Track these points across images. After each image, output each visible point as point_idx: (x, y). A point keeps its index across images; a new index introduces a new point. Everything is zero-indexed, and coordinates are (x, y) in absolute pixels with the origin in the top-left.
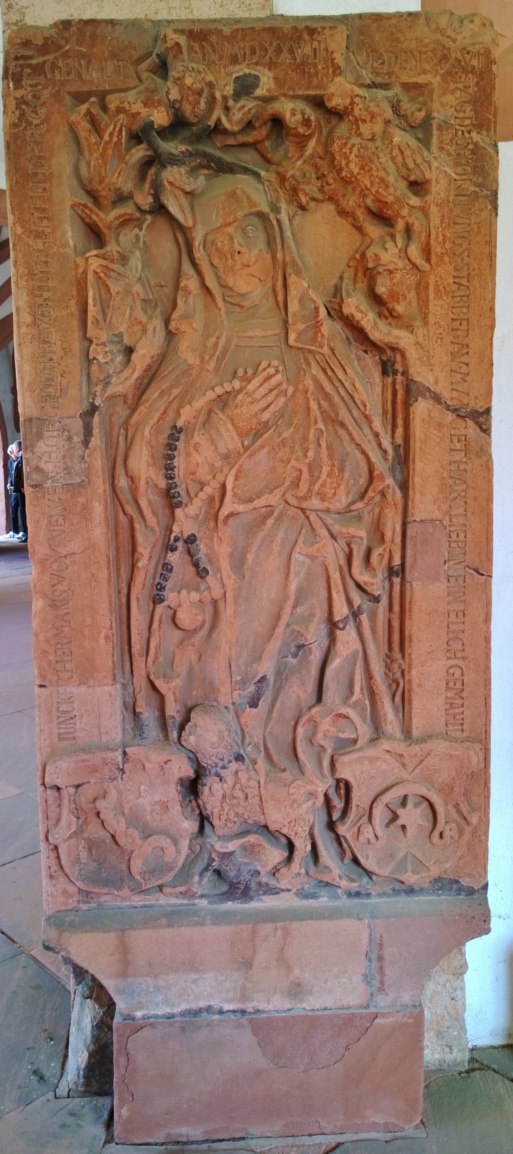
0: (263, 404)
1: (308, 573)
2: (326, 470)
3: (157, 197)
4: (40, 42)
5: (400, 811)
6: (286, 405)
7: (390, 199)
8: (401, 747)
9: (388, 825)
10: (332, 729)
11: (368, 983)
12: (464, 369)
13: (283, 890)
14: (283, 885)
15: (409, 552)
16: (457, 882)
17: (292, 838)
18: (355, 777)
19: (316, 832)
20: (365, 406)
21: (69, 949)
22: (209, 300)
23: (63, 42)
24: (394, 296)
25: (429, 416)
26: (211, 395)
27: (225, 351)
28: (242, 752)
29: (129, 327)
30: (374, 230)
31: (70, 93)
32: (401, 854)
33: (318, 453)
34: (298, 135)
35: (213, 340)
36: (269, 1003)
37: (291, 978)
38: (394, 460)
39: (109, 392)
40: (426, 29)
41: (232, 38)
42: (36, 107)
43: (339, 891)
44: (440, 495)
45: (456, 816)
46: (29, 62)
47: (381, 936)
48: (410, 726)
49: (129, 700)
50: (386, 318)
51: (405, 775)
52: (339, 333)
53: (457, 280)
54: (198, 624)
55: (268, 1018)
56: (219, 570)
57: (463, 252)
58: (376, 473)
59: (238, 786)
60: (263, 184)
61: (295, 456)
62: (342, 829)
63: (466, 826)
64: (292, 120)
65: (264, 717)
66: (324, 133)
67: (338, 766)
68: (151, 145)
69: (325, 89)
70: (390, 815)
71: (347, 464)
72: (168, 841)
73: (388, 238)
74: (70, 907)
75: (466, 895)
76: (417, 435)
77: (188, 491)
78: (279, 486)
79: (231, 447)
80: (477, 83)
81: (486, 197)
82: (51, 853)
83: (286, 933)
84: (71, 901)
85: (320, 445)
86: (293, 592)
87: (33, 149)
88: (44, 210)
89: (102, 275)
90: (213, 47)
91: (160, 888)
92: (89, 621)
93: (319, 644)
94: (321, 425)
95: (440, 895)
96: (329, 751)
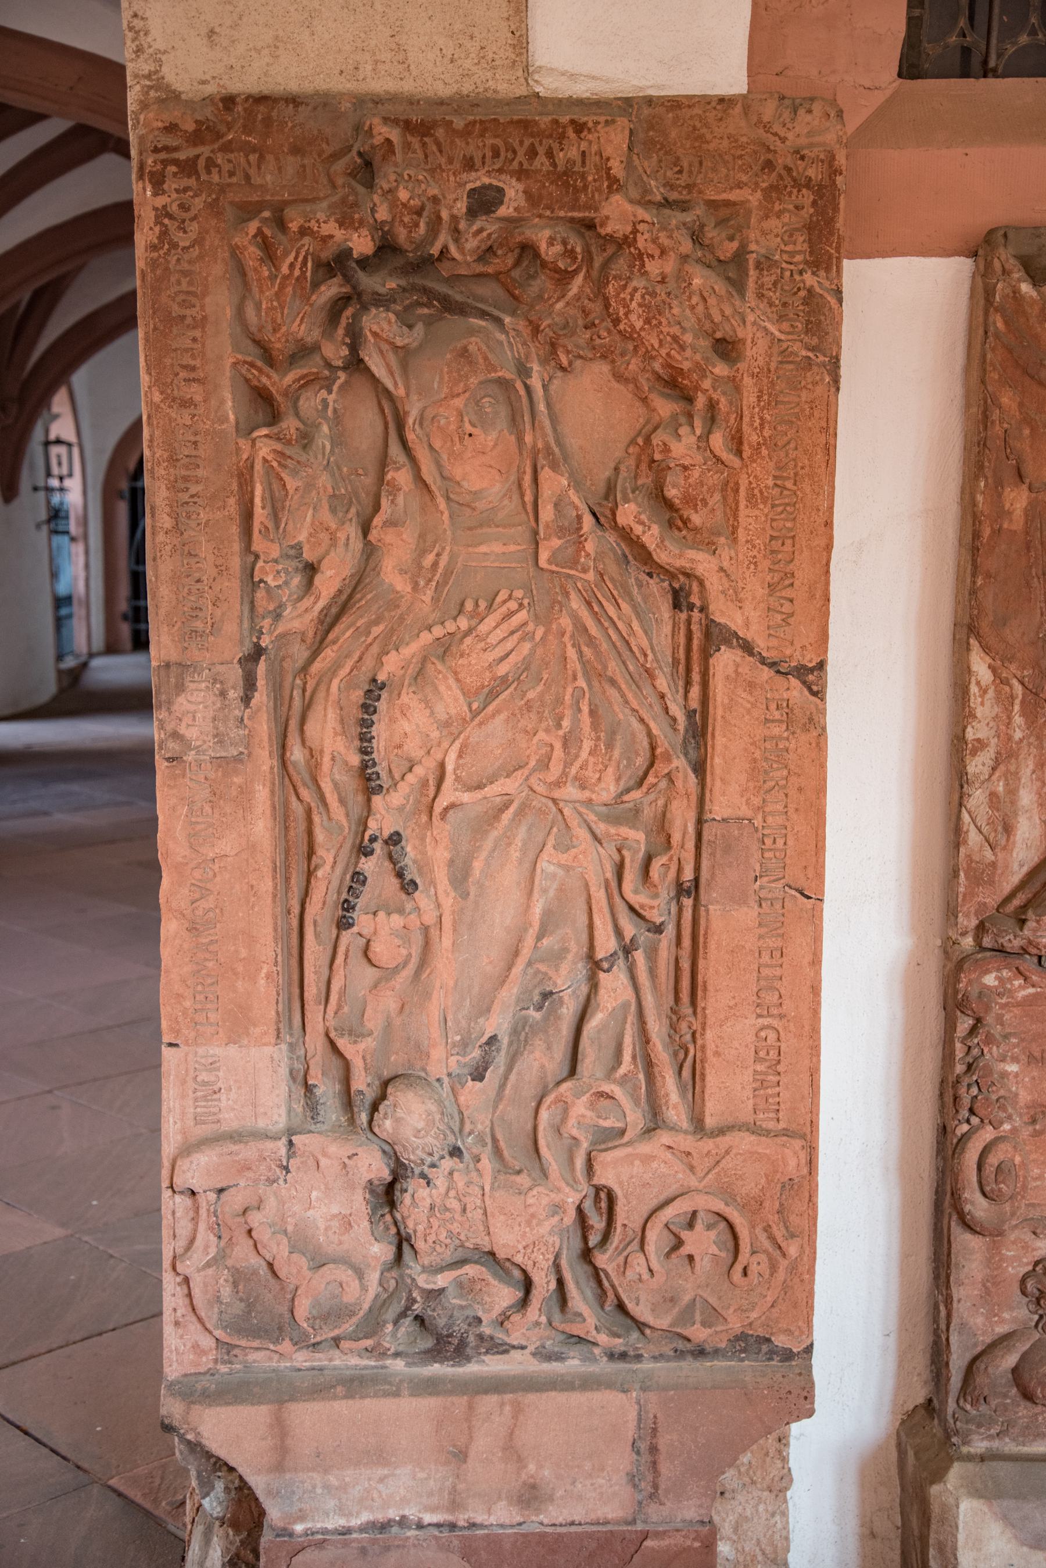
0: (499, 652)
1: (561, 890)
2: (587, 745)
3: (354, 348)
4: (190, 126)
5: (685, 1235)
6: (533, 652)
7: (686, 365)
8: (687, 1142)
9: (668, 1255)
10: (589, 1114)
11: (635, 1486)
12: (787, 607)
13: (514, 1347)
14: (514, 1339)
15: (705, 864)
17: (529, 1269)
18: (621, 1183)
19: (564, 1263)
20: (645, 655)
21: (201, 1429)
22: (427, 498)
23: (223, 129)
24: (690, 500)
25: (736, 671)
26: (426, 638)
27: (448, 573)
28: (459, 1143)
29: (311, 535)
30: (665, 407)
31: (232, 203)
32: (687, 1298)
33: (576, 722)
34: (557, 270)
35: (430, 558)
36: (490, 1515)
37: (524, 1476)
38: (687, 731)
39: (280, 629)
40: (743, 123)
41: (466, 133)
42: (183, 221)
43: (597, 1351)
44: (751, 784)
45: (767, 1244)
46: (175, 155)
47: (655, 1417)
48: (703, 1113)
49: (300, 1067)
50: (680, 530)
51: (693, 1182)
52: (612, 549)
53: (779, 482)
54: (400, 960)
55: (488, 1535)
56: (433, 883)
57: (789, 443)
58: (659, 751)
59: (452, 1193)
60: (507, 334)
61: (544, 725)
62: (601, 1260)
63: (780, 1259)
64: (550, 252)
65: (492, 1094)
66: (597, 264)
67: (597, 1167)
68: (347, 279)
69: (596, 210)
70: (671, 1241)
71: (619, 737)
72: (350, 1272)
73: (682, 420)
75: (781, 1361)
76: (719, 699)
77: (390, 771)
78: (521, 767)
79: (453, 712)
80: (814, 203)
82: (178, 1289)
83: (518, 1410)
84: (204, 1359)
85: (580, 710)
86: (538, 917)
87: (179, 283)
88: (193, 369)
89: (275, 464)
90: (439, 145)
91: (336, 1341)
92: (243, 953)
93: (574, 992)
94: (582, 683)
95: (742, 1360)
96: (585, 1145)
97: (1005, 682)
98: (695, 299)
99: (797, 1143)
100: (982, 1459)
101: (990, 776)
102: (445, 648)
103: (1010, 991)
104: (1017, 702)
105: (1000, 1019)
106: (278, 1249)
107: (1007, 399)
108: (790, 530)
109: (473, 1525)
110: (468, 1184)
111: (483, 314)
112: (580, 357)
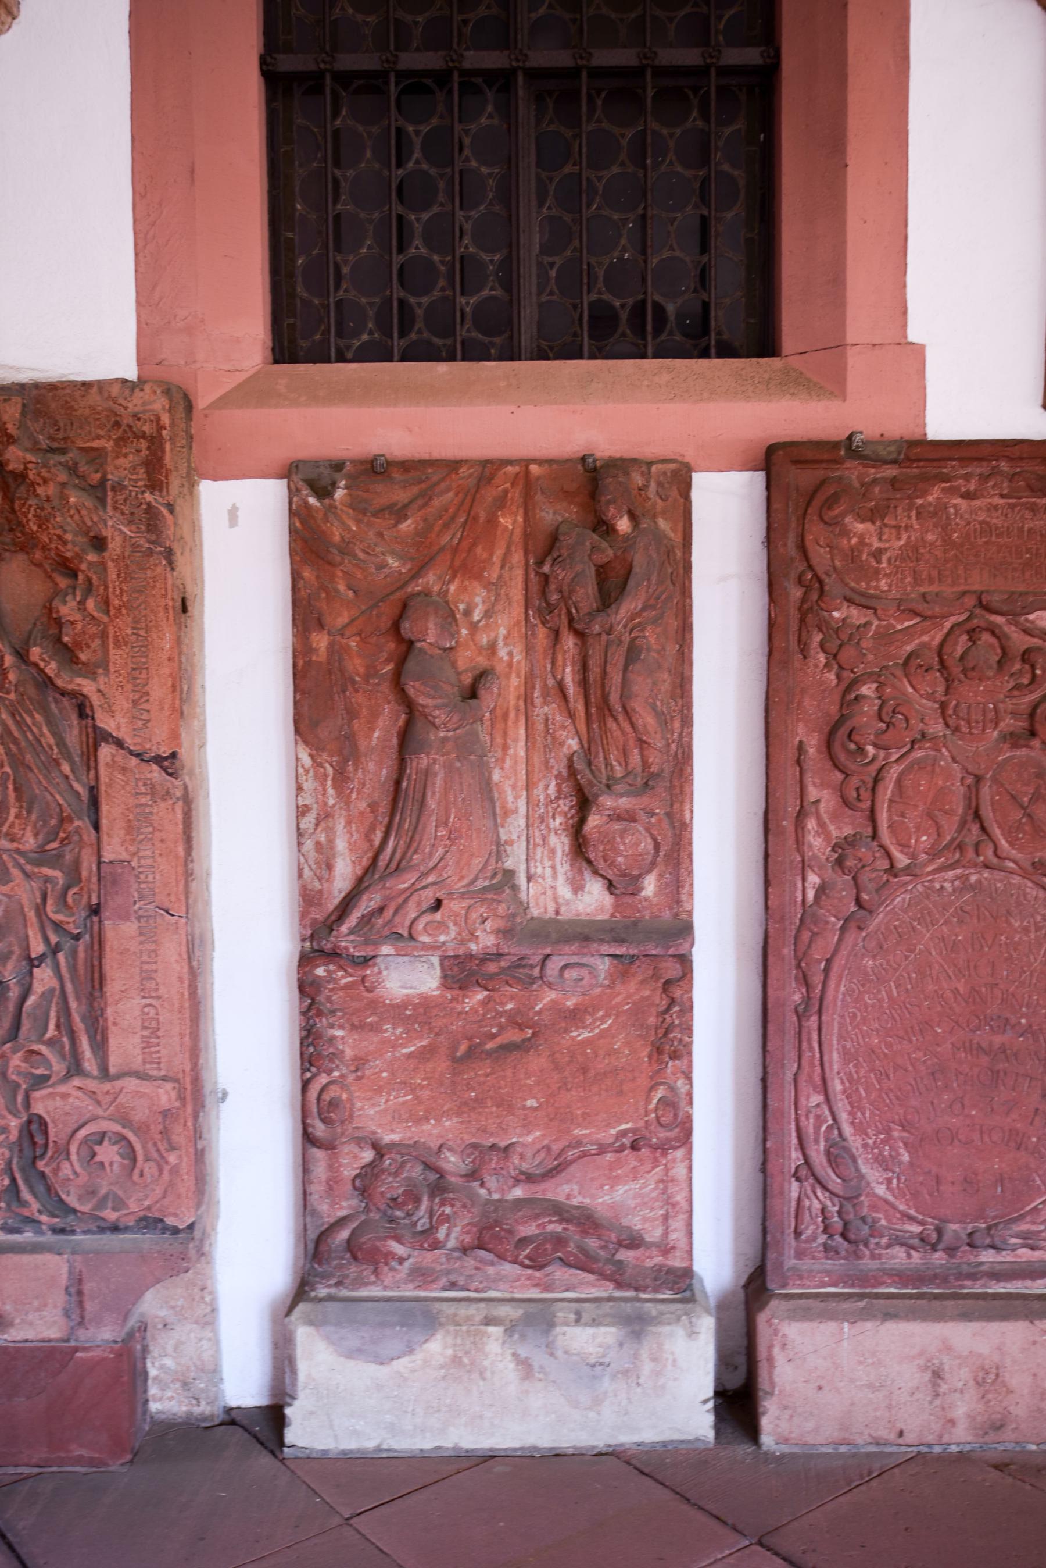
2: (13, 811)
5: (97, 1148)
7: (69, 554)
10: (23, 1065)
12: (145, 716)
16: (162, 1221)
18: (48, 1112)
19: (15, 1166)
24: (78, 645)
32: (103, 1191)
40: (98, 398)
44: (128, 837)
45: (155, 1155)
51: (100, 1112)
52: (34, 678)
57: (140, 605)
73: (70, 591)
80: (148, 448)
81: (161, 553)
85: (7, 788)
93: (18, 981)
95: (144, 1234)
96: (24, 1086)
97: (320, 765)
98: (72, 512)
99: (169, 1086)
101: (315, 829)
103: (335, 979)
104: (330, 779)
105: (329, 999)
108: (145, 663)
112: (7, 550)
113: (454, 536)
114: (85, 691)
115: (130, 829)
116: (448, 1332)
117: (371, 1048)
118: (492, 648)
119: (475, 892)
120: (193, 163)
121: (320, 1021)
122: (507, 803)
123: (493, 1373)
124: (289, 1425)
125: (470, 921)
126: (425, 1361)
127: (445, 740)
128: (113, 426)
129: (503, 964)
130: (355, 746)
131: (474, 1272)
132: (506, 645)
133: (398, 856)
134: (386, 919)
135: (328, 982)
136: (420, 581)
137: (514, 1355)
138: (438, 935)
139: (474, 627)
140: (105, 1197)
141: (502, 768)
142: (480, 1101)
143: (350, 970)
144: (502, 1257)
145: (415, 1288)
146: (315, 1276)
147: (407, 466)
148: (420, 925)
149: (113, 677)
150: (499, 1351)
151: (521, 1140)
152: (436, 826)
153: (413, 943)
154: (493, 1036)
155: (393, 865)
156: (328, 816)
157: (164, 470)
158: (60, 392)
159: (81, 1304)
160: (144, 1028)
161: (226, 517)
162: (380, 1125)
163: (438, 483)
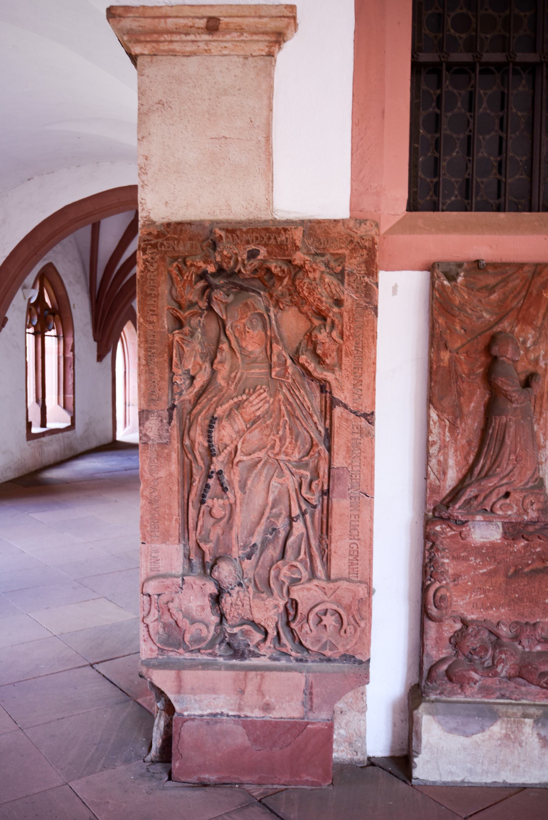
0: (257, 407)
1: (279, 492)
2: (288, 440)
4: (155, 233)
5: (323, 617)
6: (269, 407)
7: (323, 308)
8: (323, 584)
9: (317, 625)
10: (288, 573)
11: (304, 706)
12: (360, 392)
13: (262, 655)
15: (331, 483)
16: (354, 657)
17: (266, 627)
18: (299, 598)
19: (279, 626)
20: (309, 409)
22: (233, 354)
23: (166, 233)
24: (325, 355)
25: (342, 415)
26: (231, 402)
27: (240, 379)
28: (242, 582)
29: (193, 366)
31: (169, 257)
32: (324, 640)
33: (284, 432)
34: (278, 276)
35: (234, 374)
36: (252, 713)
37: (264, 701)
38: (325, 436)
39: (182, 399)
40: (343, 228)
41: (247, 232)
42: (152, 263)
43: (292, 658)
44: (347, 455)
45: (353, 622)
46: (150, 242)
48: (330, 574)
49: (187, 552)
50: (322, 365)
51: (326, 598)
54: (222, 515)
55: (252, 720)
56: (233, 488)
58: (314, 443)
59: (239, 599)
60: (262, 297)
61: (272, 433)
62: (293, 625)
63: (358, 627)
64: (276, 271)
65: (254, 564)
66: (293, 274)
67: (291, 592)
68: (207, 280)
69: (291, 256)
70: (318, 619)
71: (300, 438)
72: (204, 626)
73: (322, 327)
74: (153, 657)
77: (219, 449)
78: (264, 448)
79: (240, 428)
81: (372, 308)
83: (262, 677)
84: (154, 653)
85: (285, 428)
87: (150, 283)
88: (154, 311)
89: (180, 342)
90: (237, 236)
92: (167, 512)
94: (286, 418)
95: (344, 663)
96: (287, 584)
98: (326, 286)
99: (364, 586)
100: (433, 702)
101: (438, 454)
102: (239, 406)
105: (442, 543)
106: (179, 616)
107: (441, 320)
108: (361, 365)
109: (246, 717)
110: (244, 596)
111: (254, 291)
112: (287, 305)
113: (519, 302)
114: (329, 379)
115: (348, 450)
116: (504, 721)
117: (463, 569)
118: (537, 361)
119: (528, 489)
120: (384, 108)
121: (438, 555)
122: (540, 442)
123: (526, 743)
124: (415, 767)
125: (525, 504)
126: (490, 736)
127: (515, 409)
128: (349, 243)
129: (537, 527)
130: (461, 411)
131: (514, 689)
132: (544, 359)
133: (486, 469)
134: (479, 502)
135: (442, 534)
136: (500, 325)
137: (539, 734)
138: (507, 511)
139: (527, 350)
140: (326, 643)
141: (539, 424)
142: (520, 599)
143: (454, 528)
144: (531, 682)
145: (482, 697)
146: (429, 689)
147: (495, 265)
148: (498, 506)
149: (344, 372)
150: (530, 732)
151: (542, 620)
152: (510, 454)
153: (493, 515)
154: (529, 565)
155: (483, 474)
156: (445, 447)
157: (375, 266)
158: (323, 225)
159: (311, 699)
160: (350, 555)
161: (391, 290)
162: (466, 610)
163: (512, 275)
